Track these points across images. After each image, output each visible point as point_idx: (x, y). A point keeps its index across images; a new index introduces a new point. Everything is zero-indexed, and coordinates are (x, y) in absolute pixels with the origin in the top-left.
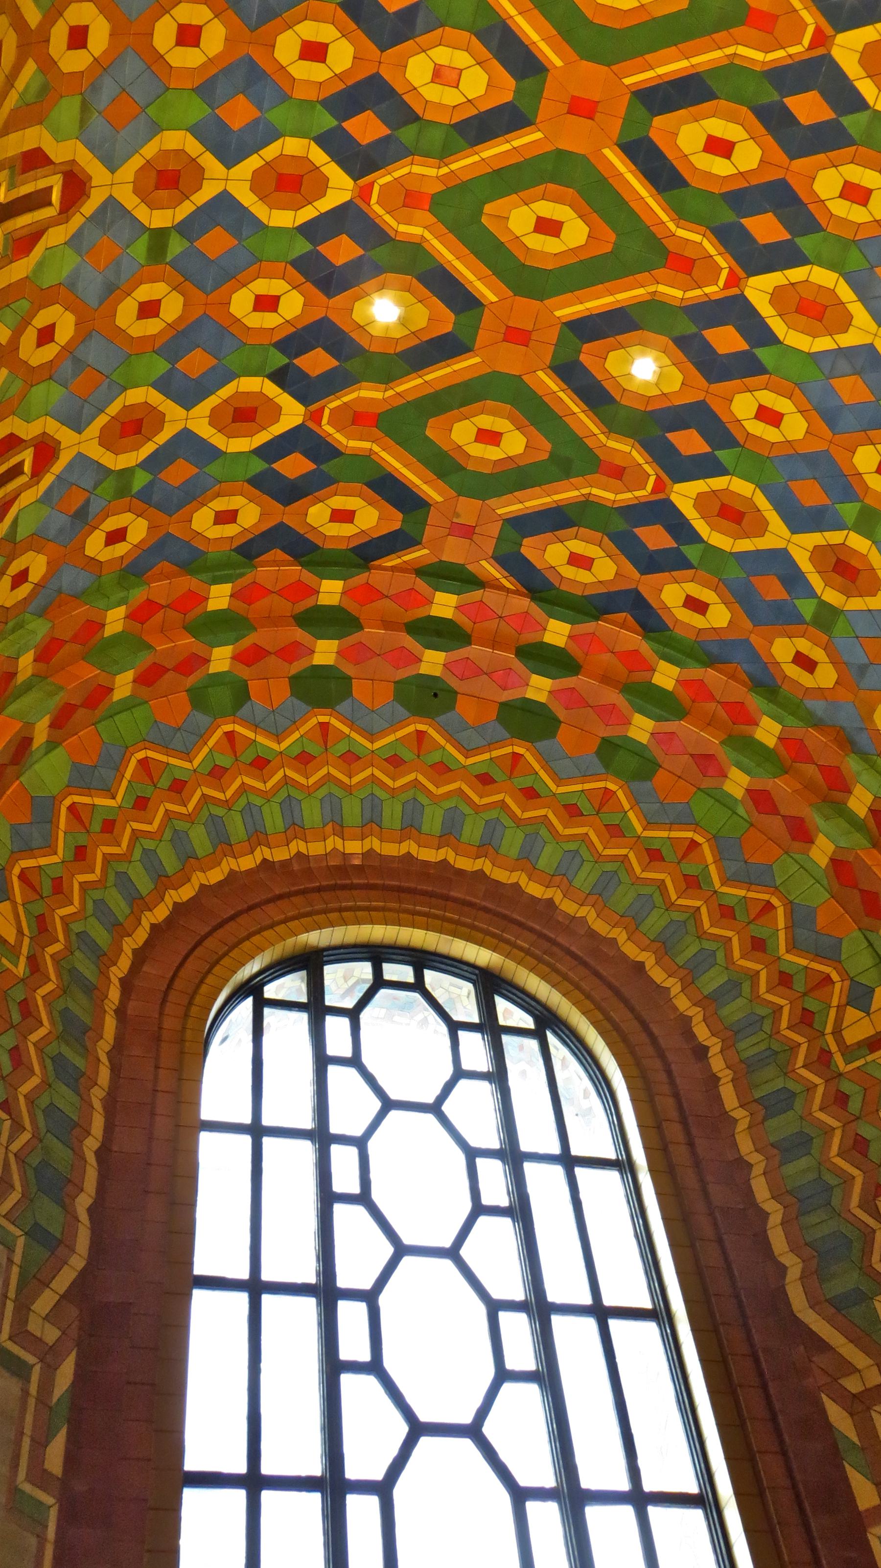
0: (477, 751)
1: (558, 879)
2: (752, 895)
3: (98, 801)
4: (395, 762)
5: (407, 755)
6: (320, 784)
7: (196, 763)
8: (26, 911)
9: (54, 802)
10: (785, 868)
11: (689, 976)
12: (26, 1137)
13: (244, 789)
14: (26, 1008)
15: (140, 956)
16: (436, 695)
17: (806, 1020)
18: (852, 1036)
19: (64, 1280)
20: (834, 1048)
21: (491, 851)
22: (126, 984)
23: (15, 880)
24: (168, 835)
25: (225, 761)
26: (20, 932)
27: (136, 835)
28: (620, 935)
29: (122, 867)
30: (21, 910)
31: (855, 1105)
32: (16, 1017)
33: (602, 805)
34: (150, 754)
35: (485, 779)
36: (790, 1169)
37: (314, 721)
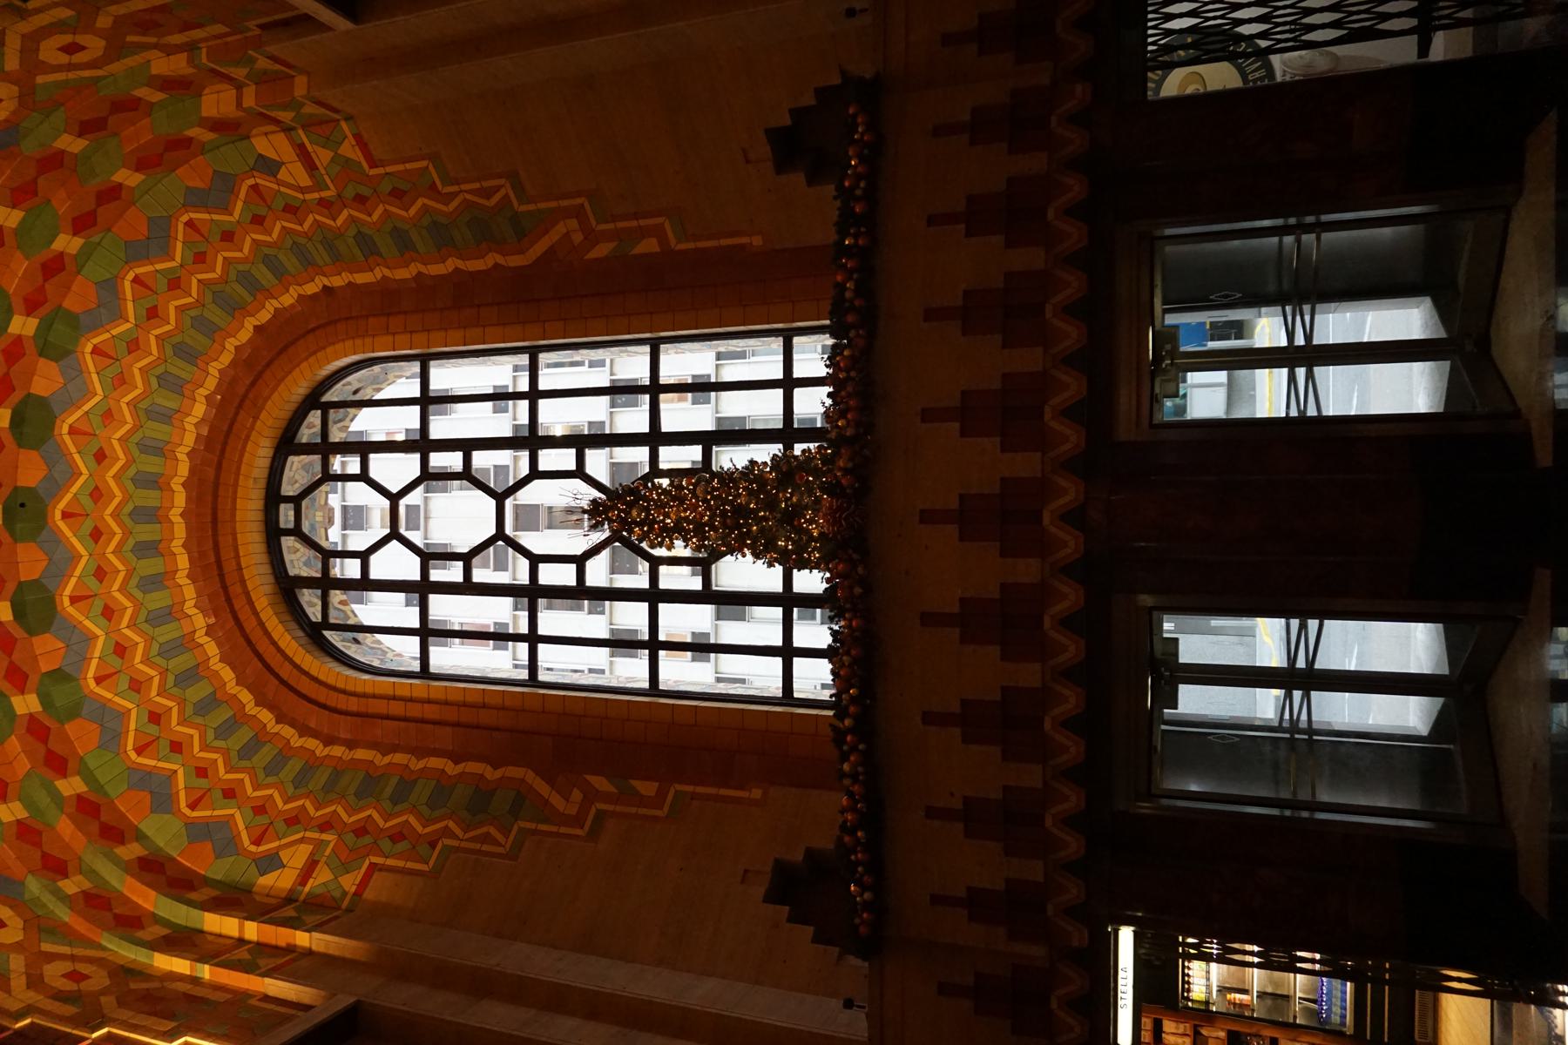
1: (186, 393)
3: (181, 785)
4: (96, 535)
5: (88, 525)
6: (130, 596)
7: (130, 706)
8: (284, 836)
9: (190, 824)
12: (451, 824)
13: (146, 660)
14: (360, 831)
15: (304, 731)
16: (22, 505)
18: (305, 181)
19: (542, 787)
20: (316, 195)
21: (169, 447)
22: (329, 741)
23: (261, 849)
24: (199, 720)
25: (123, 683)
26: (302, 841)
27: (205, 747)
28: (231, 344)
29: (234, 754)
30: (284, 841)
31: (366, 191)
32: (367, 840)
34: (130, 746)
35: (100, 456)
37: (71, 610)
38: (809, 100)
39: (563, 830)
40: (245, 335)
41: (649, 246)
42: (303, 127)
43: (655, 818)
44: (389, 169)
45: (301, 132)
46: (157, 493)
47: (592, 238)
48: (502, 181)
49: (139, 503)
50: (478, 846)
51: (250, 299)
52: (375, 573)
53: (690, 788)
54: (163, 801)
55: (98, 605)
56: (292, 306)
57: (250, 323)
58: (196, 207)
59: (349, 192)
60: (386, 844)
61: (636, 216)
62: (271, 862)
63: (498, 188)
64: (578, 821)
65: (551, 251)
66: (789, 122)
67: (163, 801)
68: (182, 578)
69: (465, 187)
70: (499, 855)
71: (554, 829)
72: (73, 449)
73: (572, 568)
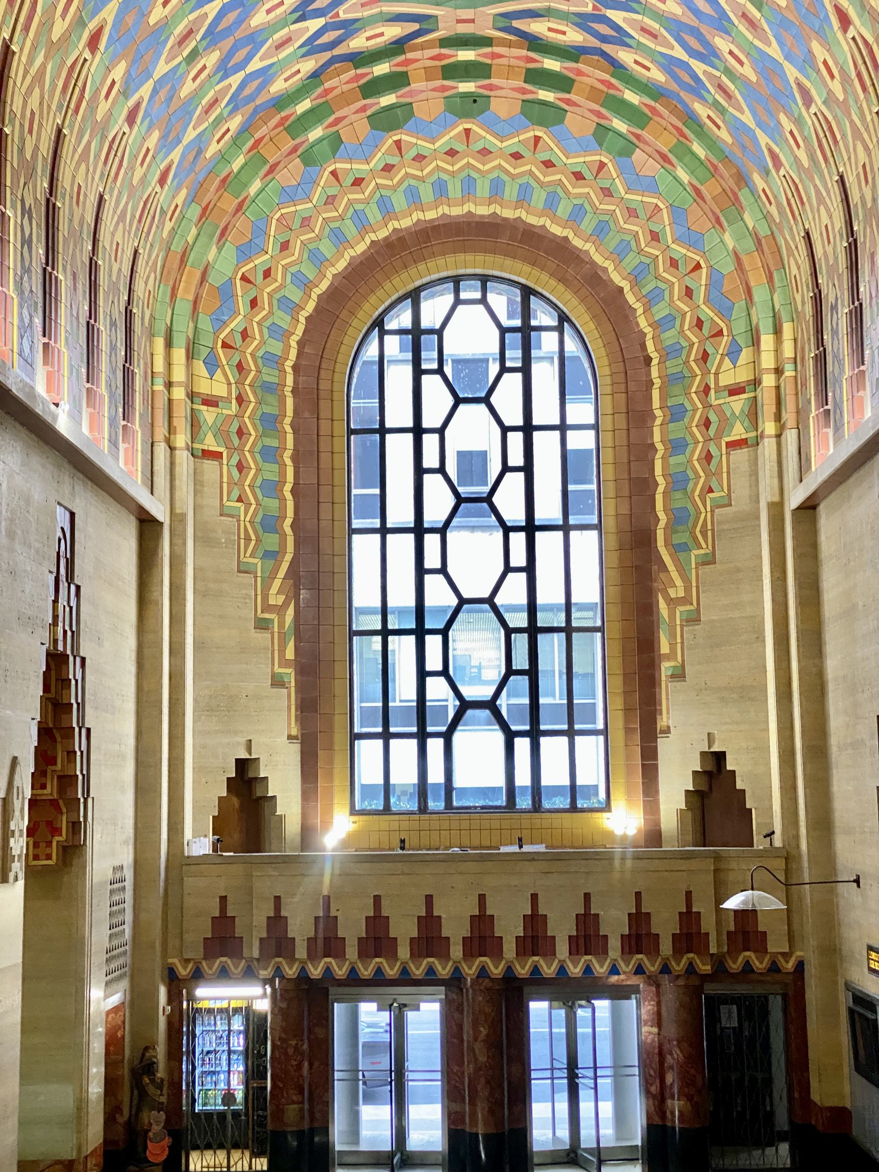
0: (510, 136)
2: (689, 254)
5: (460, 147)
10: (711, 238)
11: (649, 304)
13: (350, 203)
16: (475, 101)
26: (229, 384)
30: (226, 367)
32: (236, 441)
36: (672, 460)
39: (259, 598)
40: (617, 279)
41: (665, 648)
42: (755, 397)
43: (273, 664)
44: (724, 457)
45: (752, 395)
46: (487, 194)
47: (672, 602)
48: (710, 547)
49: (479, 183)
50: (242, 536)
53: (293, 684)
54: (245, 253)
55: (394, 160)
58: (709, 276)
59: (713, 417)
60: (235, 460)
61: (682, 643)
62: (212, 365)
64: (267, 608)
65: (665, 569)
66: (728, 768)
67: (245, 253)
68: (417, 216)
69: (709, 515)
70: (239, 556)
71: (259, 592)
72: (522, 137)
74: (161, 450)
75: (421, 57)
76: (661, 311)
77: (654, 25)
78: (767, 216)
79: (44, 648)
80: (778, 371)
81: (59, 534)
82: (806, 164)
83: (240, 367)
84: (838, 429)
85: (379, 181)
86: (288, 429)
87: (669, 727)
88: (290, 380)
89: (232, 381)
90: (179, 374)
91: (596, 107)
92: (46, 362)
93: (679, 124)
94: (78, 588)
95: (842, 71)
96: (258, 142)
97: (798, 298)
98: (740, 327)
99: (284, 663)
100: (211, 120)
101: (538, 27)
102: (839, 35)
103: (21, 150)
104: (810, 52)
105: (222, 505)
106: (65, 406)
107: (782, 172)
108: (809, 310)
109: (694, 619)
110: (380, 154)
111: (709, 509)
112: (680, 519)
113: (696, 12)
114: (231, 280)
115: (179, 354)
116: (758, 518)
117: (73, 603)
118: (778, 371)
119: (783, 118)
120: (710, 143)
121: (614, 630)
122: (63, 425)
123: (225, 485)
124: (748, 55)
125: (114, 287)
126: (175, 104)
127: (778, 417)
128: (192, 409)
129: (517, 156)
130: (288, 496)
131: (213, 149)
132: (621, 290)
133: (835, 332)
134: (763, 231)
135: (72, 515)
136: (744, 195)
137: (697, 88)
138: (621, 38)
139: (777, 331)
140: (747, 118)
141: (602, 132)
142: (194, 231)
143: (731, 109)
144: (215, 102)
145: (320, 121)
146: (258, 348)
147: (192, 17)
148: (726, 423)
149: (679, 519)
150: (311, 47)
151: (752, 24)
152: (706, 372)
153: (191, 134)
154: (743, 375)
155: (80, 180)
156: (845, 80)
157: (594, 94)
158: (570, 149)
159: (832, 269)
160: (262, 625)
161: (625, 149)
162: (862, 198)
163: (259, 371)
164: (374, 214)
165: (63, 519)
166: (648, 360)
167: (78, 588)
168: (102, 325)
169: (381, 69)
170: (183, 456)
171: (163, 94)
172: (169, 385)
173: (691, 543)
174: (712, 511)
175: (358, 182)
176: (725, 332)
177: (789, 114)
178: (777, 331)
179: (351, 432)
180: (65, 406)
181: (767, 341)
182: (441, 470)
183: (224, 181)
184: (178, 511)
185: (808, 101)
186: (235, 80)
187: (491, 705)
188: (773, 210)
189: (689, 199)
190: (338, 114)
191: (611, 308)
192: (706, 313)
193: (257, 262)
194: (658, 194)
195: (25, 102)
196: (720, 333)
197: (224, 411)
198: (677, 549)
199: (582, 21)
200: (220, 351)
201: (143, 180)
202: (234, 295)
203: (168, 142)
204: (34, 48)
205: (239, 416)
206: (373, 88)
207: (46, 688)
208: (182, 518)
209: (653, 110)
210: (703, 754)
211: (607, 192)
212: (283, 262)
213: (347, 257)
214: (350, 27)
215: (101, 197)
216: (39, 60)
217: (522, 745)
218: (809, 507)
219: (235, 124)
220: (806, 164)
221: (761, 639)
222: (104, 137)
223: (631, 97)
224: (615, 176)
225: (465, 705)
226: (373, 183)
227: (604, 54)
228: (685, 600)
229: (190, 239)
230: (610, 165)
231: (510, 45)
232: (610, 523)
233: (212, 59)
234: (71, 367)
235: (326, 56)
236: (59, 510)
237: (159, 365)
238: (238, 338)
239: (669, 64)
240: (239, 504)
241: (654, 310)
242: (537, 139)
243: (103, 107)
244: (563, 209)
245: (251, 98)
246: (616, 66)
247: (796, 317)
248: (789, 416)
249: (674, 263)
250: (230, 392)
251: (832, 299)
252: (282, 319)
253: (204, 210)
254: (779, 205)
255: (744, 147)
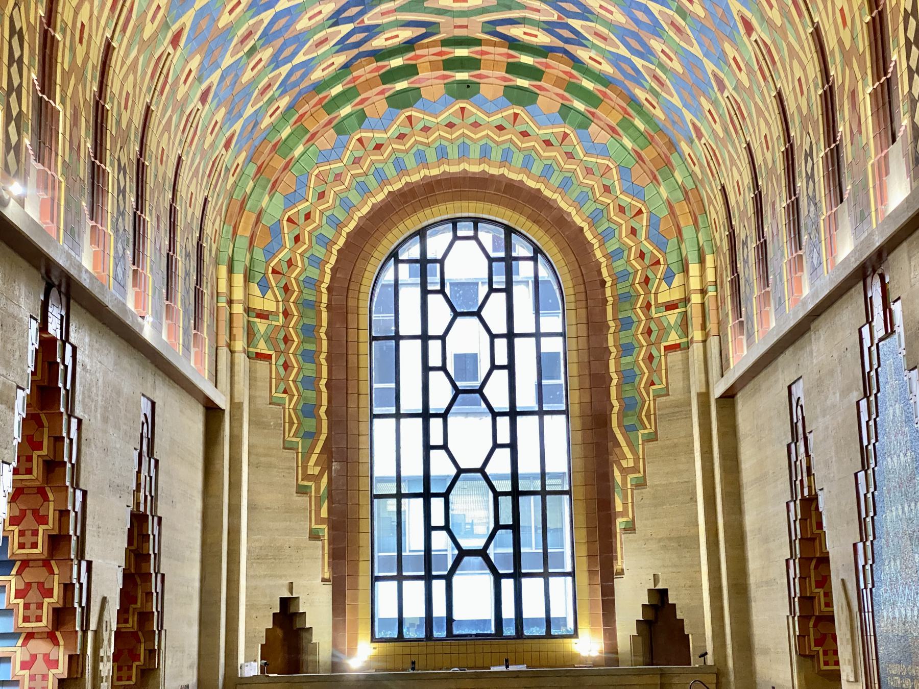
0: (495, 113)
10: (650, 192)
13: (372, 162)
17: (647, 280)
19: (320, 444)
21: (507, 164)
26: (278, 301)
28: (573, 212)
30: (275, 289)
32: (282, 346)
33: (563, 140)
36: (624, 360)
38: (679, 616)
39: (300, 469)
40: (578, 221)
41: (619, 507)
42: (686, 312)
44: (663, 358)
46: (477, 156)
47: (624, 471)
48: (653, 428)
51: (600, 230)
52: (430, 297)
53: (326, 537)
54: (291, 200)
56: (595, 256)
57: (585, 226)
59: (653, 327)
61: (632, 503)
62: (264, 287)
63: (650, 423)
64: (306, 477)
66: (670, 602)
67: (291, 200)
68: (424, 172)
69: (652, 402)
72: (504, 114)
73: (440, 442)
74: (224, 353)
75: (426, 54)
76: (612, 246)
77: (604, 31)
78: (692, 174)
79: (129, 509)
80: (703, 292)
81: (143, 419)
82: (721, 134)
83: (286, 289)
84: (750, 336)
85: (395, 146)
86: (324, 336)
87: (623, 570)
88: (325, 299)
89: (280, 299)
90: (238, 294)
91: (561, 92)
92: (134, 286)
93: (624, 105)
94: (157, 462)
95: (747, 64)
96: (302, 116)
97: (717, 236)
98: (673, 258)
99: (319, 520)
100: (265, 99)
101: (516, 32)
102: (745, 38)
103: (119, 122)
104: (723, 51)
105: (271, 396)
106: (149, 319)
107: (703, 141)
108: (725, 246)
109: (641, 484)
110: (395, 126)
111: (651, 398)
112: (630, 406)
113: (637, 21)
114: (280, 222)
115: (239, 279)
116: (690, 404)
117: (153, 474)
118: (703, 292)
119: (702, 100)
120: (648, 118)
121: (579, 493)
122: (148, 333)
123: (274, 380)
124: (676, 53)
125: (189, 226)
126: (238, 88)
127: (704, 327)
128: (248, 321)
129: (500, 128)
130: (323, 389)
131: (266, 121)
132: (582, 229)
133: (746, 262)
134: (690, 185)
135: (153, 404)
136: (675, 159)
137: (637, 77)
138: (579, 40)
139: (702, 261)
140: (676, 101)
141: (566, 111)
142: (251, 184)
143: (663, 94)
144: (269, 86)
145: (349, 100)
146: (300, 274)
147: (251, 22)
148: (664, 331)
149: (629, 406)
150: (343, 45)
151: (678, 30)
152: (648, 293)
153: (249, 111)
154: (676, 295)
155: (164, 144)
156: (750, 72)
157: (558, 82)
158: (541, 122)
159: (743, 214)
160: (302, 491)
161: (583, 123)
162: (765, 160)
163: (301, 292)
164: (390, 171)
165: (146, 407)
166: (603, 283)
167: (157, 462)
168: (179, 257)
169: (396, 62)
170: (241, 360)
171: (228, 81)
172: (230, 302)
173: (638, 425)
174: (654, 400)
175: (378, 147)
176: (662, 262)
177: (708, 98)
178: (702, 261)
179: (373, 339)
180: (149, 319)
181: (694, 269)
182: (443, 368)
183: (275, 145)
184: (236, 401)
185: (722, 87)
186: (285, 70)
187: (482, 553)
188: (697, 169)
189: (631, 162)
190: (363, 96)
191: (575, 244)
192: (648, 247)
193: (300, 208)
194: (609, 157)
195: (122, 85)
196: (658, 262)
197: (274, 323)
198: (629, 430)
199: (549, 27)
200: (270, 275)
201: (213, 145)
202: (281, 232)
203: (233, 115)
204: (130, 46)
205: (285, 326)
206: (391, 76)
207: (130, 542)
208: (240, 405)
209: (605, 94)
210: (649, 590)
211: (570, 156)
212: (320, 208)
213: (370, 204)
214: (372, 31)
215: (180, 158)
216: (134, 53)
217: (508, 585)
218: (729, 396)
219: (284, 103)
220: (721, 134)
221: (694, 499)
222: (183, 112)
223: (588, 84)
224: (575, 143)
225: (463, 553)
226: (390, 148)
227: (566, 52)
228: (635, 469)
229: (248, 190)
230: (572, 135)
231: (495, 44)
232: (575, 409)
233: (266, 54)
234: (154, 288)
235: (355, 52)
236: (143, 400)
237: (223, 287)
238: (285, 266)
239: (616, 61)
240: (285, 395)
241: (607, 245)
242: (516, 115)
243: (182, 90)
244: (537, 169)
245: (296, 84)
246: (576, 62)
247: (716, 251)
248: (712, 326)
249: (622, 209)
250: (278, 308)
251: (743, 237)
252: (320, 252)
253: (260, 168)
254: (701, 166)
255: (674, 122)
